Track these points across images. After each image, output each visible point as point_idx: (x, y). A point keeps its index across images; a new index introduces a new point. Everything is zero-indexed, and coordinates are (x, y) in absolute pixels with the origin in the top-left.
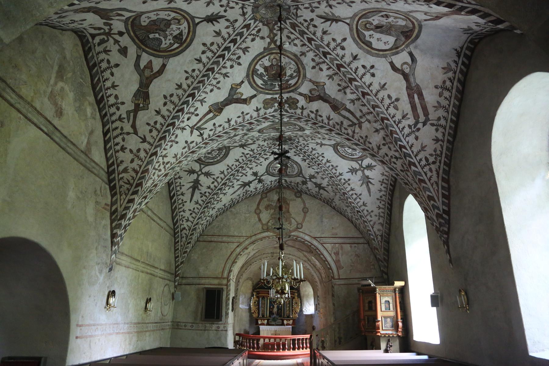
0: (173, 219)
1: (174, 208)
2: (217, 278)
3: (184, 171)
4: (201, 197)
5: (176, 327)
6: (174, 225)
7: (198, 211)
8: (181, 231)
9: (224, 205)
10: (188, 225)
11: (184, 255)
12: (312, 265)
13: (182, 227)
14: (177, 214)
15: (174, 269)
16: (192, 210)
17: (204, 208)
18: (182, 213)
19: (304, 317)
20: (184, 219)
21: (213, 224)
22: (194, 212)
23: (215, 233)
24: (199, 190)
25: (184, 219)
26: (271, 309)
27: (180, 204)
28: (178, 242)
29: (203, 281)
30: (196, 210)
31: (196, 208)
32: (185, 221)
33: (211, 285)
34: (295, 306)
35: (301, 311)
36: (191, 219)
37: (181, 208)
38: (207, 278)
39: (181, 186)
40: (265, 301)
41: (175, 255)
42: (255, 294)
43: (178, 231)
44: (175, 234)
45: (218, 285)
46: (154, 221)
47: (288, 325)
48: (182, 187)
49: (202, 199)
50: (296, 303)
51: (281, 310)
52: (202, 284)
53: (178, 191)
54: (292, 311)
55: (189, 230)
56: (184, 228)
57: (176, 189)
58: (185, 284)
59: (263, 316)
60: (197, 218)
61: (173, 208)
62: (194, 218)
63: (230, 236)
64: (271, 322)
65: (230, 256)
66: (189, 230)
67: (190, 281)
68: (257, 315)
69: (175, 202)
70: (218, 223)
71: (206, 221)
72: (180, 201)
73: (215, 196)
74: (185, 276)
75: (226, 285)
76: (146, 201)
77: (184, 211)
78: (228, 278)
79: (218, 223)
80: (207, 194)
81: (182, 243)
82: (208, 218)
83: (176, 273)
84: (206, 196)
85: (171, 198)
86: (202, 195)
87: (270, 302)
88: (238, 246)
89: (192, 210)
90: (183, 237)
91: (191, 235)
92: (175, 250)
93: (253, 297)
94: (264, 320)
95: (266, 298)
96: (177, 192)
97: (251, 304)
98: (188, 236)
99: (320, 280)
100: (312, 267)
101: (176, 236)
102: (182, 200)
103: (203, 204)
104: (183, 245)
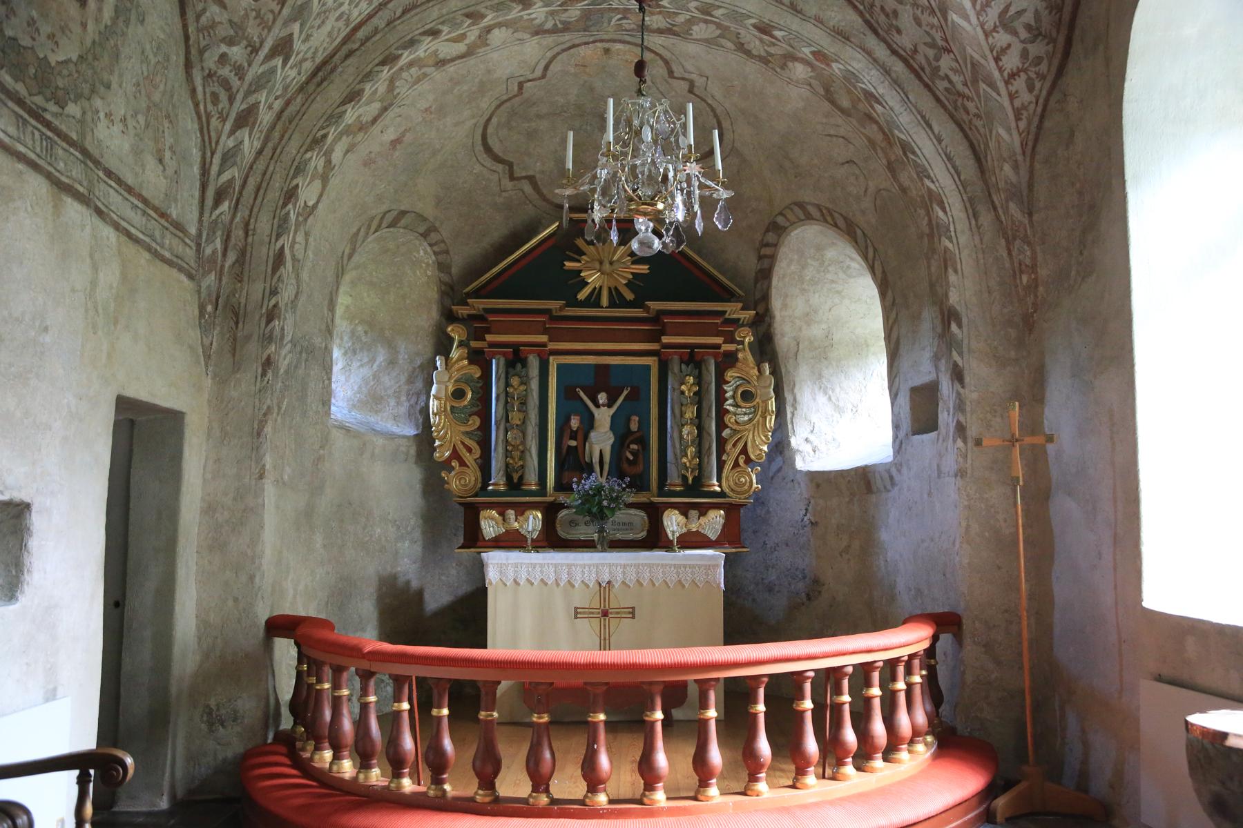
12: (899, 67)
19: (803, 490)
26: (574, 436)
34: (738, 415)
35: (781, 447)
40: (525, 382)
42: (456, 333)
47: (692, 541)
50: (747, 396)
51: (643, 442)
54: (721, 450)
59: (515, 485)
64: (572, 523)
68: (472, 477)
87: (567, 393)
93: (446, 353)
94: (521, 509)
95: (534, 362)
97: (433, 405)
99: (963, 185)
100: (896, 83)
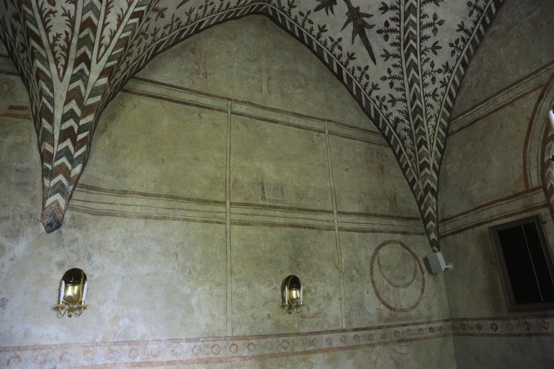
0: (367, 112)
1: (357, 93)
2: (516, 195)
3: (315, 11)
4: (386, 38)
5: (462, 331)
6: (376, 122)
7: (400, 70)
8: (395, 128)
9: (461, 28)
10: (400, 111)
11: (423, 174)
13: (392, 118)
14: (367, 101)
15: (417, 207)
16: (388, 75)
17: (407, 56)
18: (375, 94)
20: (385, 103)
21: (466, 85)
22: (394, 77)
23: (475, 100)
24: (371, 27)
25: (385, 103)
27: (361, 78)
28: (401, 151)
29: (485, 214)
30: (396, 72)
31: (392, 68)
32: (389, 105)
33: (506, 217)
36: (398, 95)
37: (366, 85)
38: (492, 203)
39: (337, 43)
41: (408, 180)
43: (390, 130)
44: (388, 139)
45: (525, 211)
46: (276, 122)
48: (340, 44)
49: (390, 41)
52: (486, 222)
53: (341, 56)
55: (408, 118)
56: (397, 120)
57: (335, 55)
58: (453, 233)
60: (407, 86)
61: (355, 93)
62: (401, 90)
63: (511, 85)
65: (529, 130)
66: (408, 118)
67: (461, 222)
69: (350, 80)
70: (476, 76)
71: (438, 84)
72: (358, 73)
73: (412, 17)
74: (446, 216)
75: (546, 206)
76: (97, 68)
77: (375, 87)
78: (544, 187)
79: (476, 76)
80: (393, 25)
81: (409, 151)
82: (440, 77)
83: (422, 215)
84: (394, 31)
85: (339, 76)
86: (385, 32)
88: (541, 97)
89: (388, 75)
90: (405, 138)
91: (416, 127)
92: (404, 171)
96: (339, 59)
98: (411, 132)
101: (392, 142)
102: (359, 69)
103: (399, 50)
104: (412, 154)
